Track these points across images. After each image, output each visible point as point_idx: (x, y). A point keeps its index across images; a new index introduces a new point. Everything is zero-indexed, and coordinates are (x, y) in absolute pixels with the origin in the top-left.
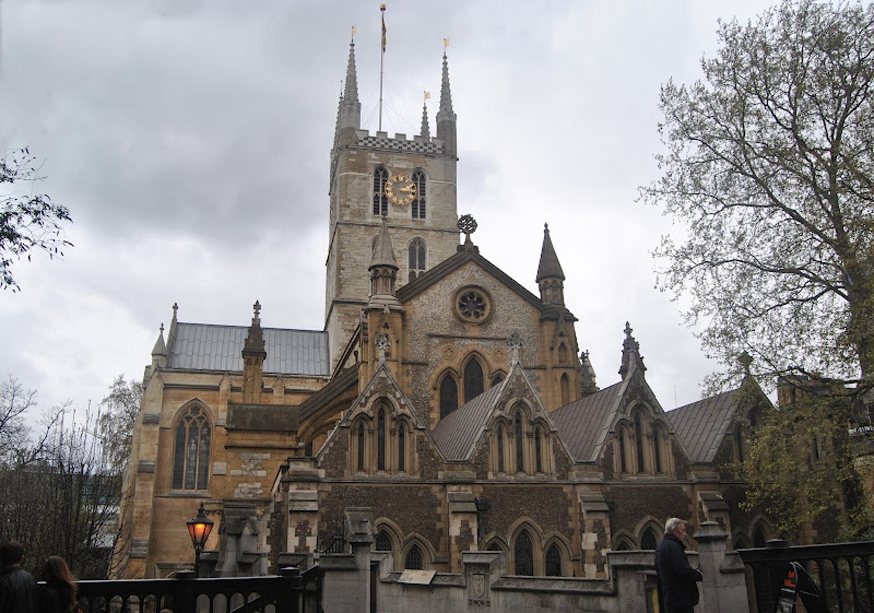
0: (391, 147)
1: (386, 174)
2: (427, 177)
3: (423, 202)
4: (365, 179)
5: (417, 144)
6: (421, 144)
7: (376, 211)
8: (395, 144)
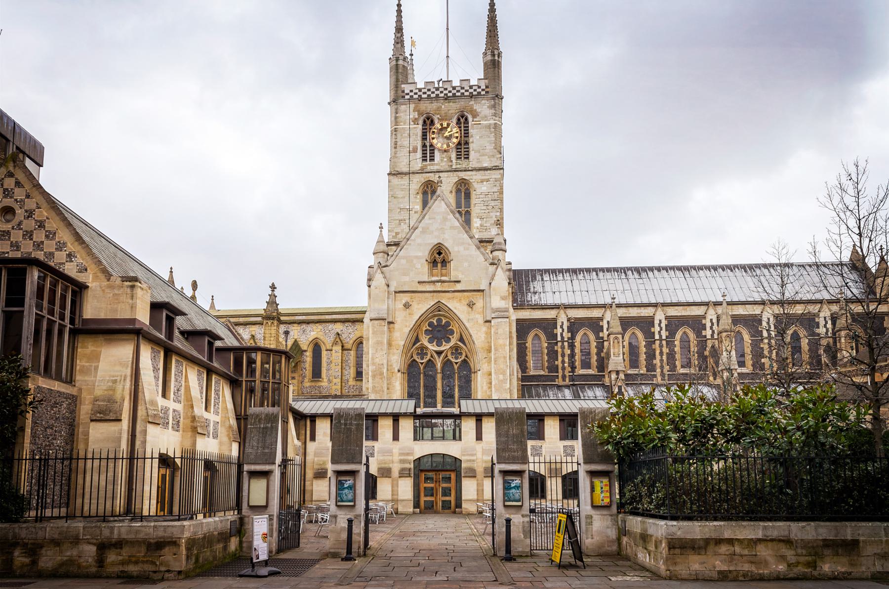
3: (467, 143)
5: (463, 88)
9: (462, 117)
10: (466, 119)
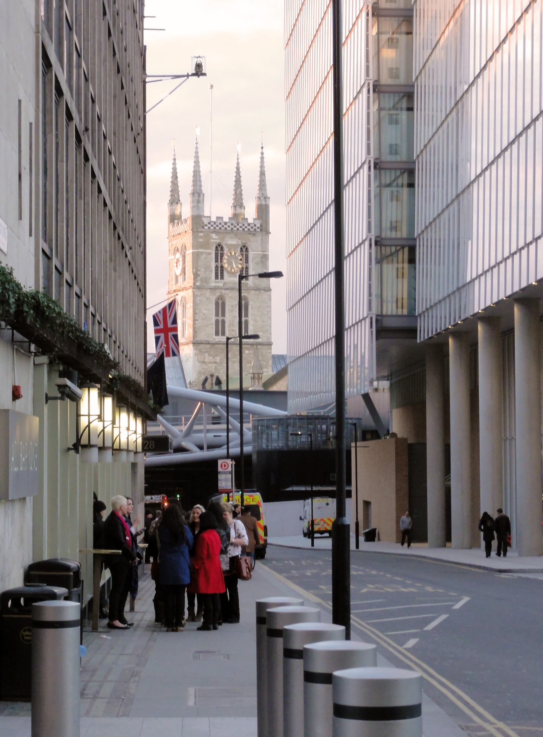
0: (226, 228)
1: (222, 249)
2: (250, 250)
4: (210, 254)
6: (246, 225)
7: (217, 277)
8: (229, 226)
10: (247, 249)
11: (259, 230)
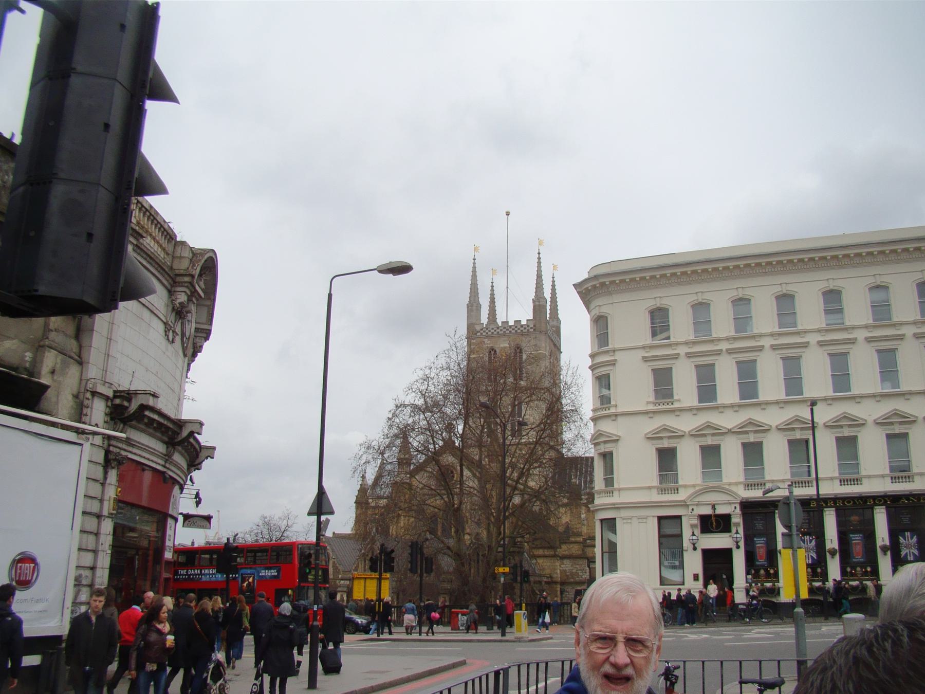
0: (498, 332)
5: (516, 327)
6: (519, 327)
8: (501, 330)
9: (518, 348)
11: (532, 330)
